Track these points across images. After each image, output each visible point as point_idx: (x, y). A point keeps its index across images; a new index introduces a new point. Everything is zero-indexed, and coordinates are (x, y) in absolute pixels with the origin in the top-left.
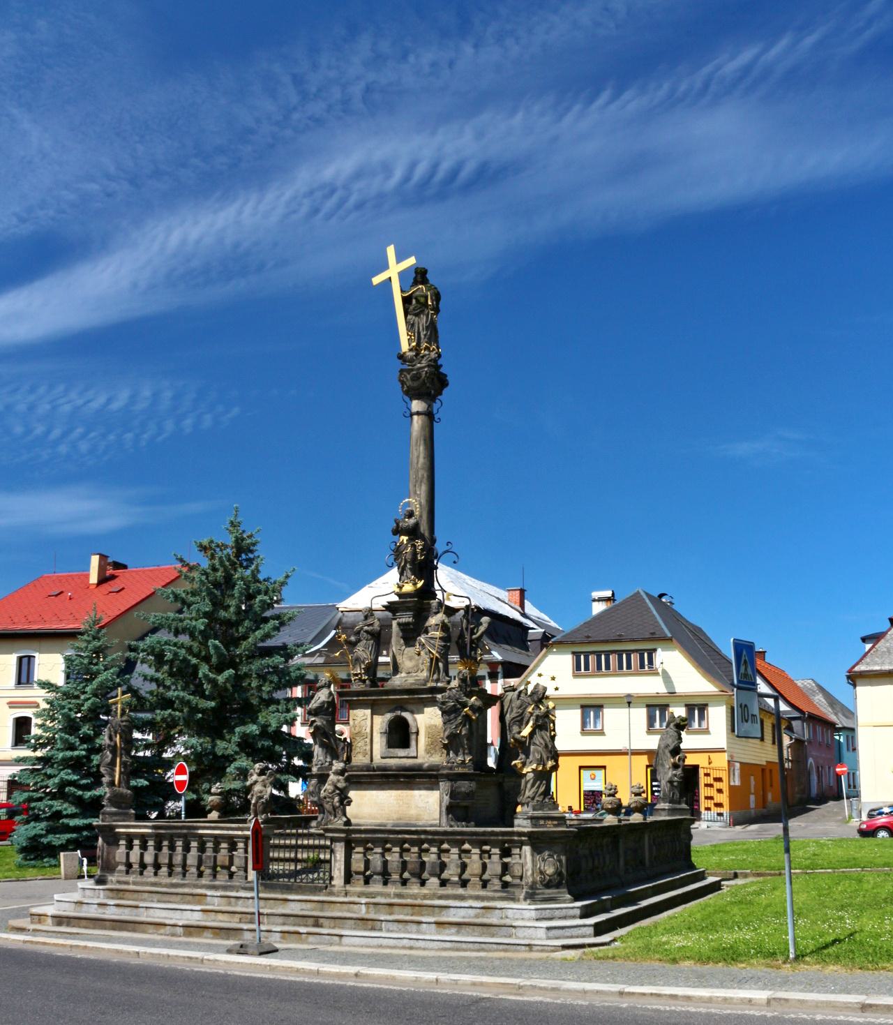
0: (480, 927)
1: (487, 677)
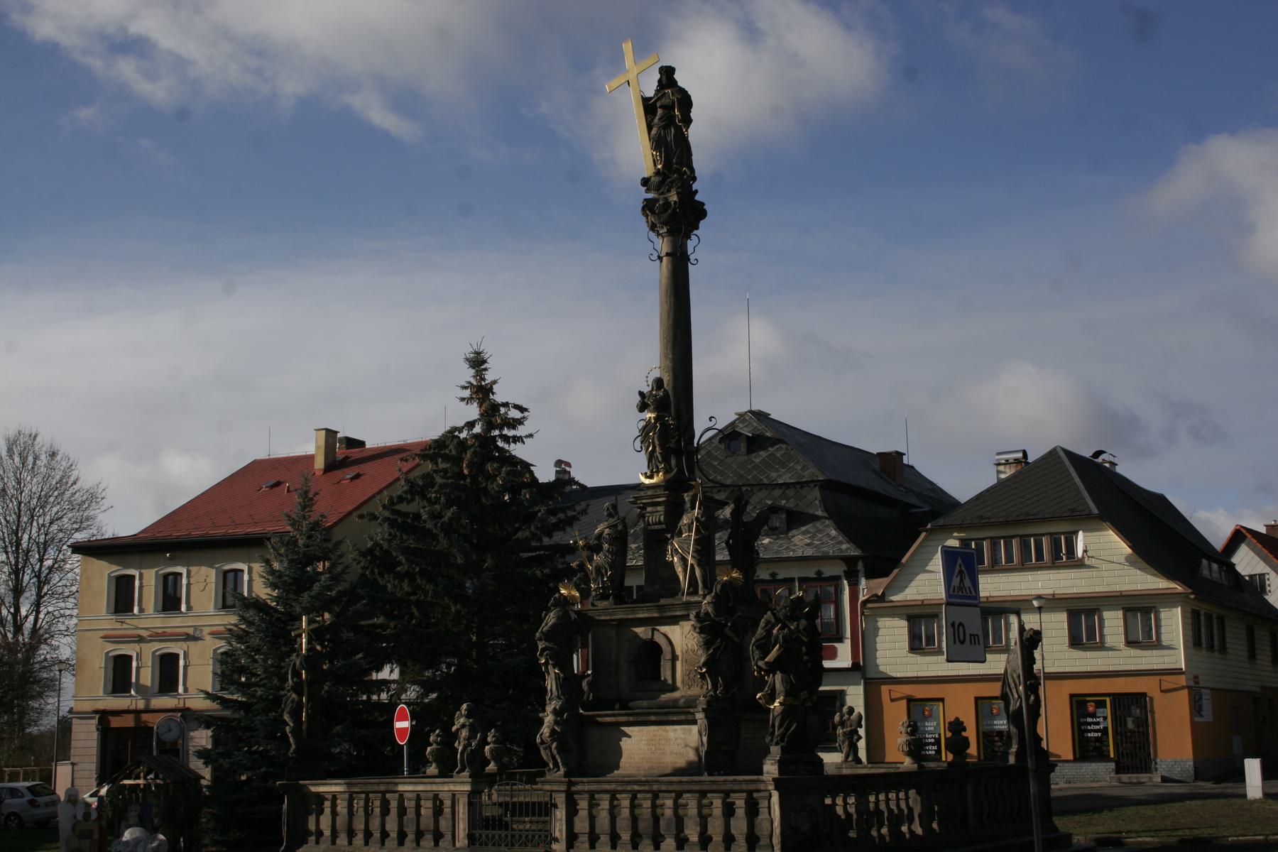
1: (843, 577)
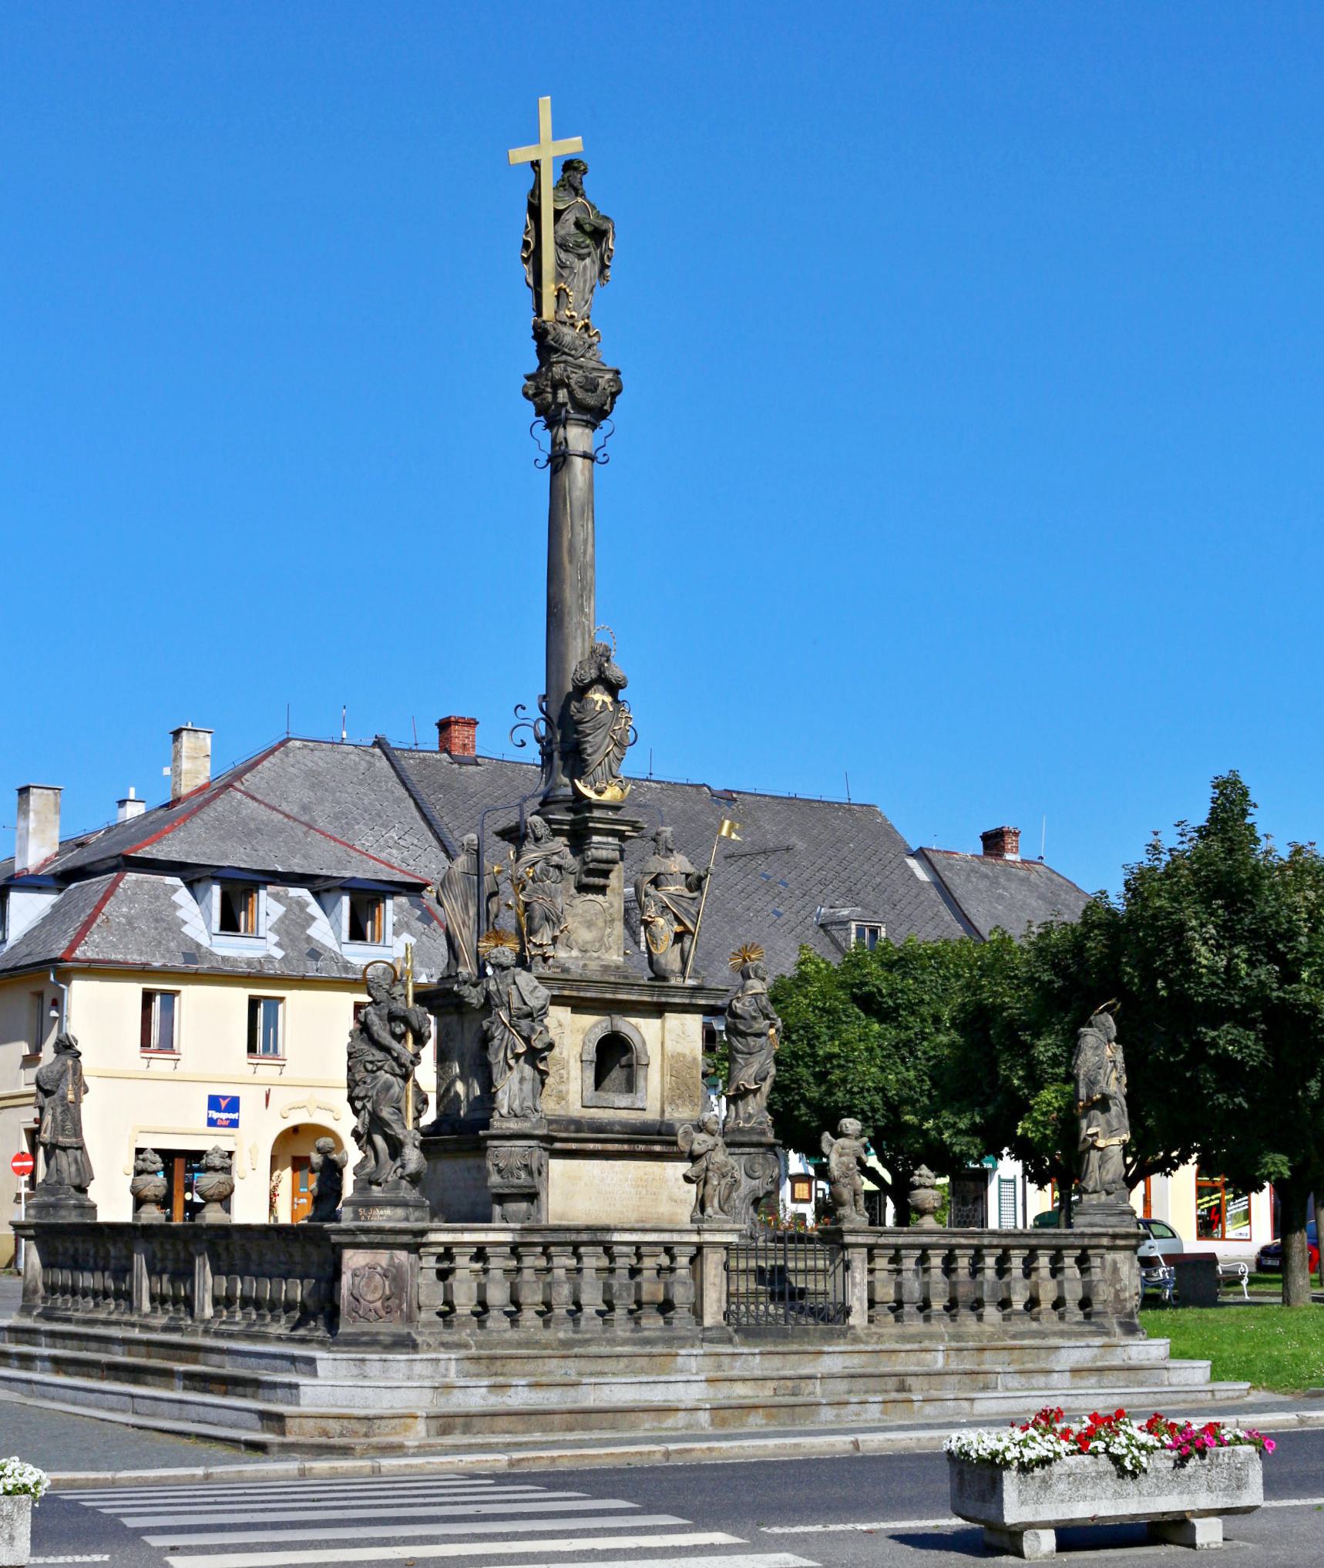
0: (1127, 1372)
